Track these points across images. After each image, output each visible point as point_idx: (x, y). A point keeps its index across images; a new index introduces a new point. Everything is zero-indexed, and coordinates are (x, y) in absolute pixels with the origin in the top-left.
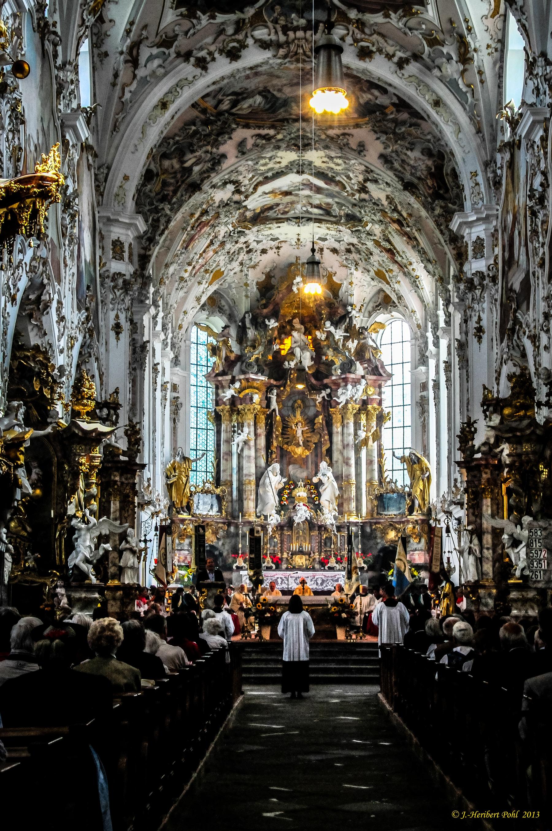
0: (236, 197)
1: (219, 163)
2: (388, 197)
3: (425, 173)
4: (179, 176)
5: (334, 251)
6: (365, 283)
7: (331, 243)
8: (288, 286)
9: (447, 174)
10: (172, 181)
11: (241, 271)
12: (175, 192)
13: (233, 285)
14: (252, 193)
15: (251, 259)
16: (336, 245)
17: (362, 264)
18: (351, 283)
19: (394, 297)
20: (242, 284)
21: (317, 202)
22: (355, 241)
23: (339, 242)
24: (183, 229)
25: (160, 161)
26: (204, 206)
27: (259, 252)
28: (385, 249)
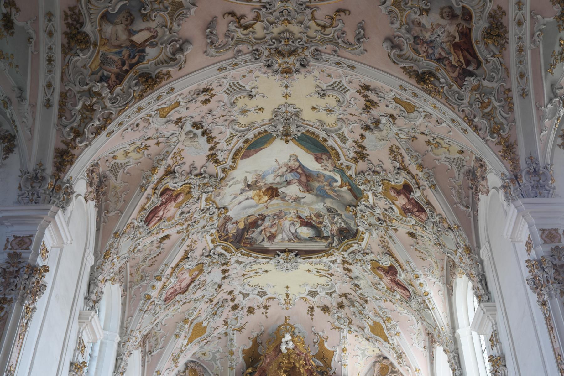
0: (212, 168)
1: (181, 50)
2: (391, 150)
3: (446, 46)
4: (125, 53)
5: (326, 309)
6: (359, 352)
7: (322, 299)
8: (277, 347)
9: (477, 42)
10: (116, 58)
11: (226, 334)
12: (120, 78)
13: (218, 355)
14: (232, 168)
15: (236, 319)
16: (327, 301)
17: (356, 320)
18: (344, 350)
19: (393, 358)
20: (227, 354)
21: (305, 213)
22: (347, 288)
23: (330, 294)
24: (142, 187)
25: (100, 26)
26: (170, 161)
27: (245, 310)
28: (383, 269)
